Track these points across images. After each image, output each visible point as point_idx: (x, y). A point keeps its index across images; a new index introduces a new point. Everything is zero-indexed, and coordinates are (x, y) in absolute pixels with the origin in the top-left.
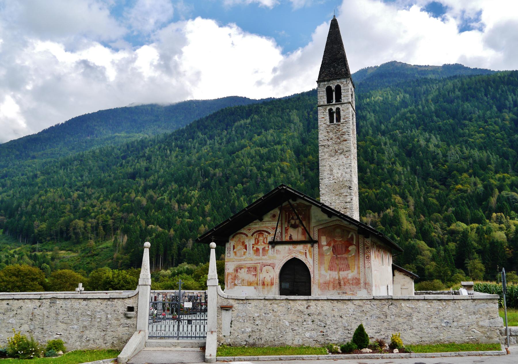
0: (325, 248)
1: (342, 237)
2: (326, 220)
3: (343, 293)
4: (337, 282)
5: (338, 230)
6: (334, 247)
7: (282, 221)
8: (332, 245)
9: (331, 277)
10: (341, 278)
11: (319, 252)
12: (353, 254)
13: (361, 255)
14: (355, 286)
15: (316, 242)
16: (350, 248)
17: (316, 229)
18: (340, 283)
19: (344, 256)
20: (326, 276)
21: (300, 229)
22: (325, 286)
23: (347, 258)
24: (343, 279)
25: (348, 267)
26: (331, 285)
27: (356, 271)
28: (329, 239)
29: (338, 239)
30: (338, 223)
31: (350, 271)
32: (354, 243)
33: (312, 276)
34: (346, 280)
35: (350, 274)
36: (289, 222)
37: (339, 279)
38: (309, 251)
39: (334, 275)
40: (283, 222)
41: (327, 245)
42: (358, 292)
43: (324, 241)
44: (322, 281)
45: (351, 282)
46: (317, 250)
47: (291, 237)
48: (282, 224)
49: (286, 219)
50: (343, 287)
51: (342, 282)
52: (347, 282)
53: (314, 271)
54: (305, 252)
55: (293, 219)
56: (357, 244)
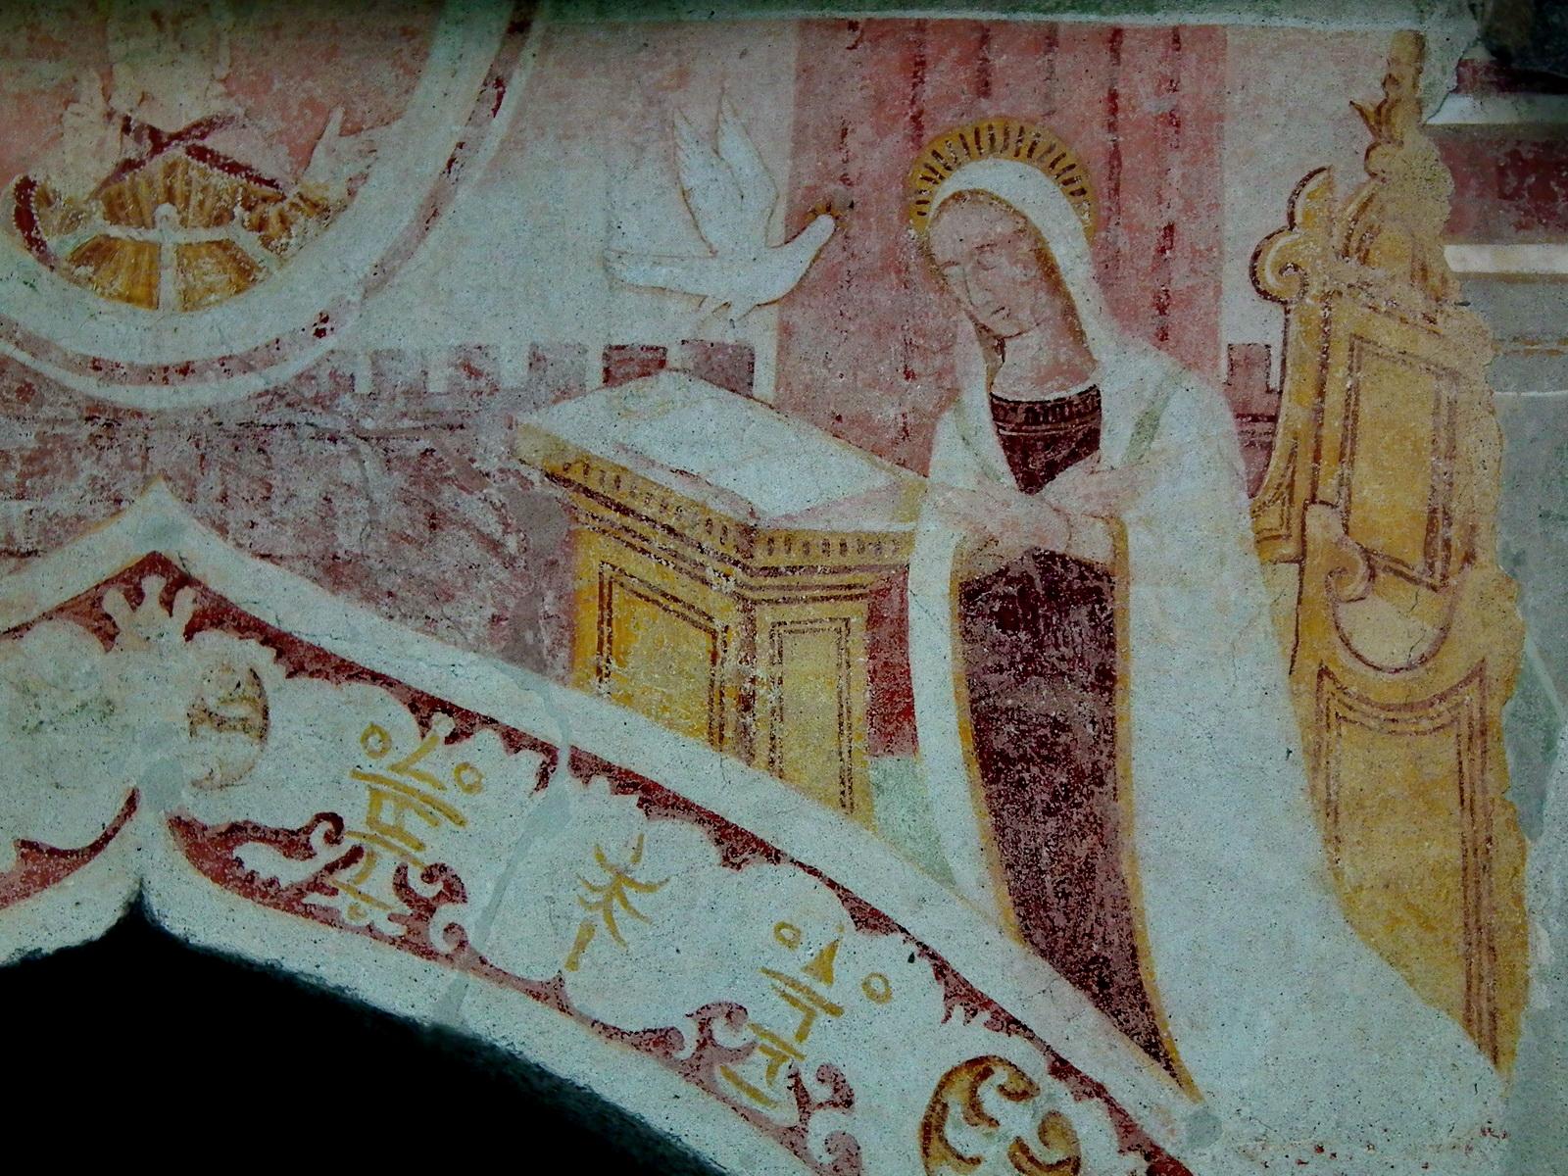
38: (1285, 454)
54: (962, 508)
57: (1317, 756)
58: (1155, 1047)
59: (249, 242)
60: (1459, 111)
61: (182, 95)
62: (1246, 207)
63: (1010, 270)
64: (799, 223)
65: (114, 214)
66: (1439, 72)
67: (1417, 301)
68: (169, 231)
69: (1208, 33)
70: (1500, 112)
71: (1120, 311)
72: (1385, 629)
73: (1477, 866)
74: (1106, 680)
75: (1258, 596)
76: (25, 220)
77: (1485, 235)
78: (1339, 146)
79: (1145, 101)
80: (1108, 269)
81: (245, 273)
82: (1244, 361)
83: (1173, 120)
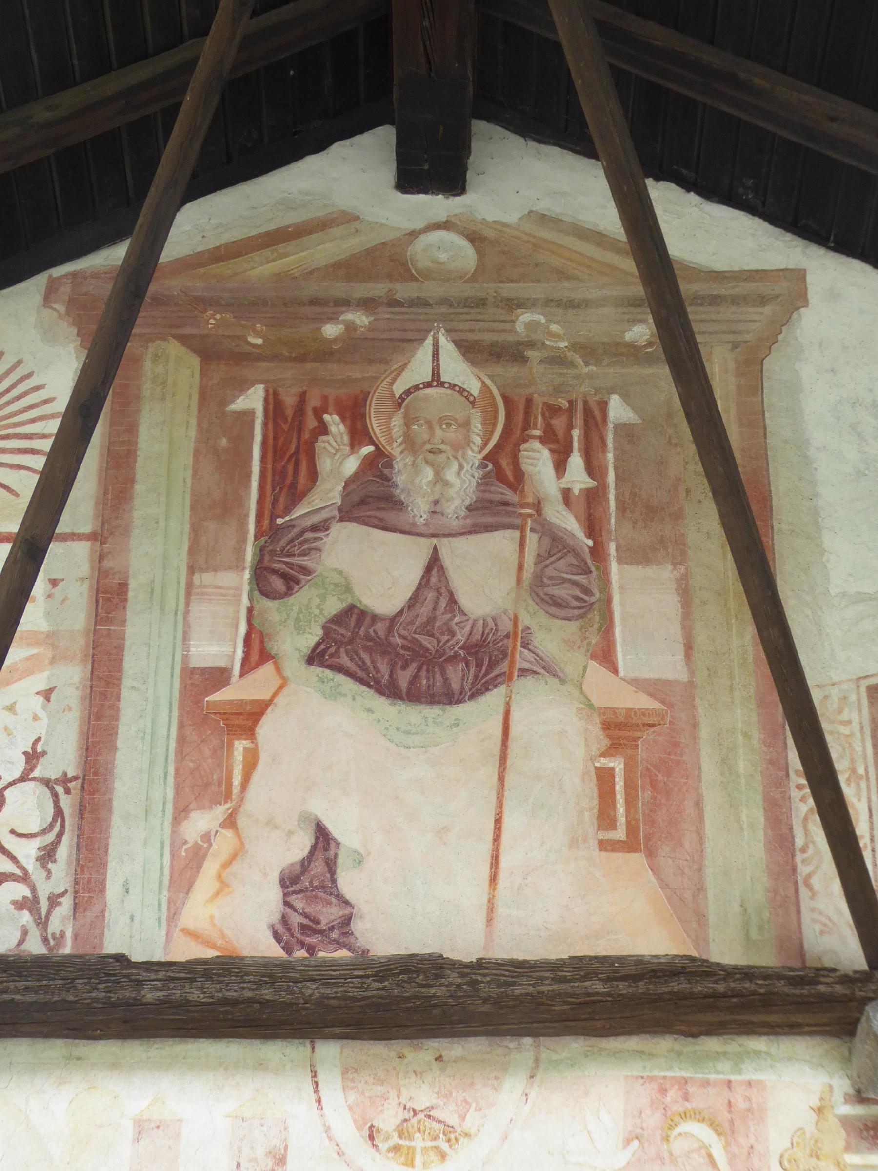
7: (109, 532)
21: (550, 724)
36: (279, 572)
40: (155, 548)
47: (316, 871)
48: (109, 597)
49: (212, 509)
55: (374, 500)
59: (445, 1146)
61: (422, 1095)
63: (699, 1159)
64: (628, 1141)
65: (400, 1136)
66: (838, 1096)
68: (419, 1142)
69: (760, 1082)
76: (371, 1138)
77: (858, 1151)
81: (443, 1156)
83: (749, 1110)
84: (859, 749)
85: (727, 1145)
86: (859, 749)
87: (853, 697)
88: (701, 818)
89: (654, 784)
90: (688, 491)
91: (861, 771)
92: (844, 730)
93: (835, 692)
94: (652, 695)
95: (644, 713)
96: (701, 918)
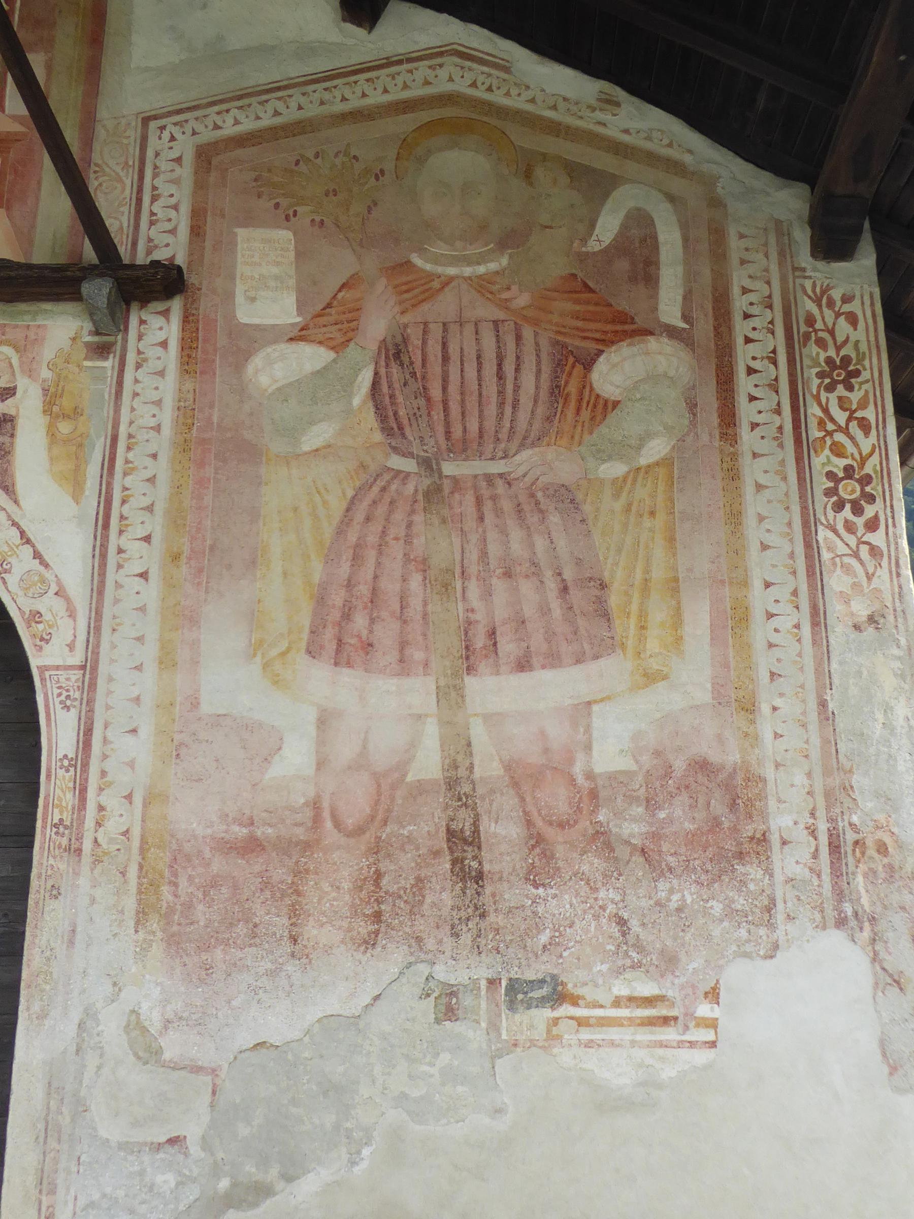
0: (280, 368)
1: (509, 241)
2: (307, 50)
3: (517, 993)
4: (427, 825)
5: (459, 162)
6: (395, 351)
8: (377, 325)
9: (345, 750)
10: (487, 766)
11: (187, 414)
12: (657, 449)
13: (764, 461)
14: (687, 893)
15: (161, 283)
16: (614, 372)
17: (175, 147)
18: (463, 843)
19: (525, 461)
20: (261, 743)
22: (242, 887)
23: (567, 498)
24: (520, 778)
25: (587, 615)
26: (343, 865)
27: (693, 678)
28: (341, 262)
29: (458, 264)
30: (451, 79)
31: (612, 671)
32: (670, 311)
33: (58, 734)
34: (559, 800)
35: (614, 716)
37: (457, 785)
39: (390, 716)
41: (301, 335)
42: (736, 975)
43: (264, 279)
44: (196, 816)
45: (632, 828)
46: (169, 387)
50: (514, 893)
51: (502, 832)
52: (572, 821)
53: (89, 668)
56: (704, 328)
57: (50, 449)
58: (16, 502)
60: (89, 339)
62: (48, 353)
66: (85, 332)
67: (77, 370)
70: (96, 339)
71: (23, 371)
72: (64, 428)
73: (77, 469)
74: (12, 436)
75: (41, 421)
77: (91, 360)
78: (66, 344)
79: (32, 336)
80: (21, 364)
82: (44, 381)
84: (132, 152)
85: (21, 357)
86: (132, 152)
87: (134, 124)
88: (39, 190)
89: (16, 172)
90: (60, 12)
91: (131, 163)
92: (125, 141)
93: (124, 121)
94: (21, 124)
95: (16, 133)
96: (31, 242)
